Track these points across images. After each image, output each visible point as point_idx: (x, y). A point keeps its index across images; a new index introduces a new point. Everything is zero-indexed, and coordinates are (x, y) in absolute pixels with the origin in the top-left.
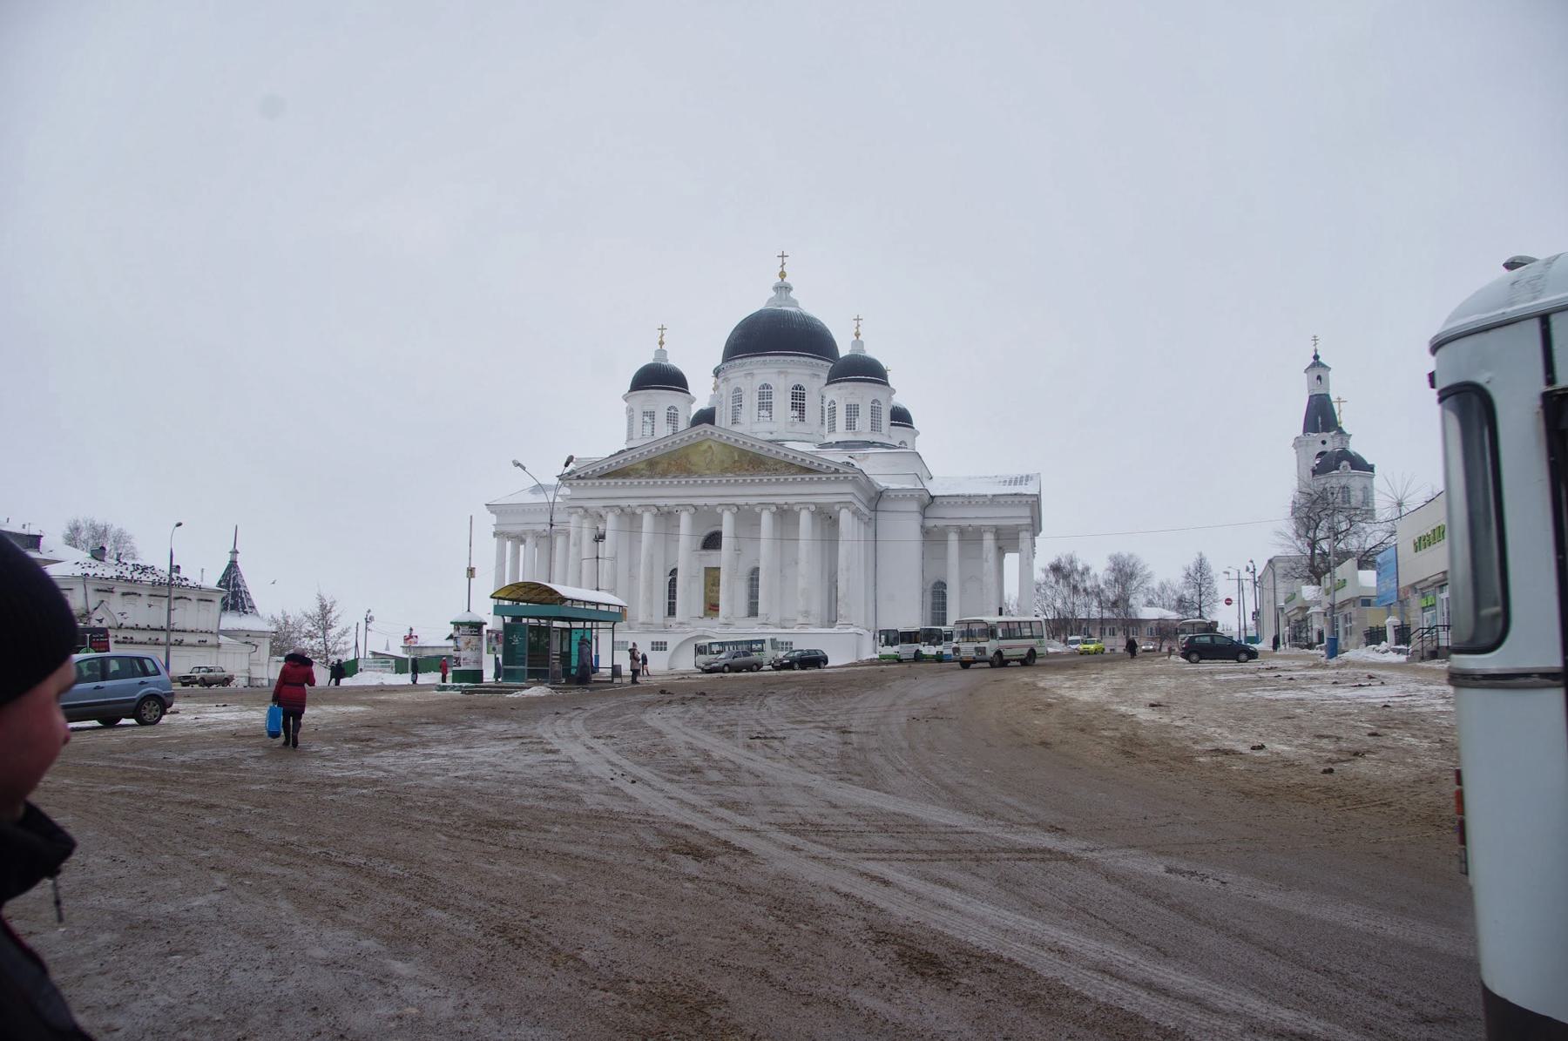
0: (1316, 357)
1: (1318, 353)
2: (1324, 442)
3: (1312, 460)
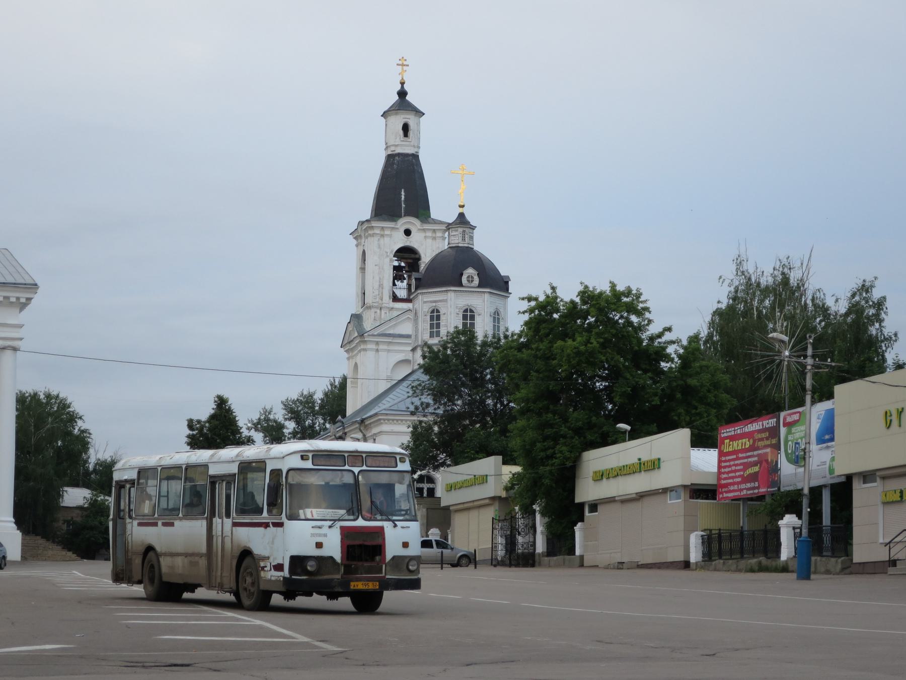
0: (402, 94)
2: (408, 233)
3: (388, 260)
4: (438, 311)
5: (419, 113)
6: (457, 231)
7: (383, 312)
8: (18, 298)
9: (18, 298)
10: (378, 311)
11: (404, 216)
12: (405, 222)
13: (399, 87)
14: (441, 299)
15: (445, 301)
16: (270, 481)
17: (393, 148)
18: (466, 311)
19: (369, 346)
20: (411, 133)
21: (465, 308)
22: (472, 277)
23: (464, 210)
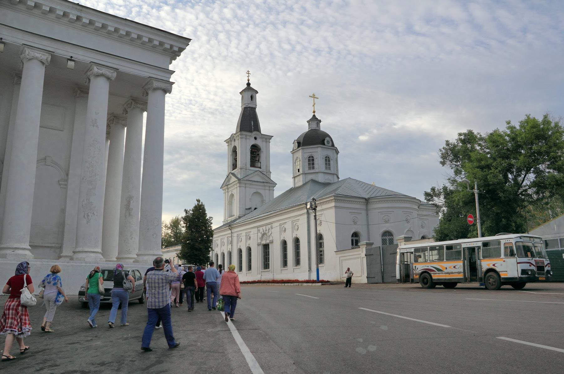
0: (249, 84)
1: (250, 82)
4: (312, 157)
5: (257, 92)
6: (315, 122)
7: (247, 171)
8: (172, 46)
9: (172, 46)
10: (245, 170)
11: (254, 131)
12: (255, 134)
13: (247, 82)
14: (313, 151)
15: (317, 152)
16: (118, 254)
17: (247, 105)
18: (326, 157)
19: (242, 185)
20: (254, 99)
21: (326, 156)
22: (329, 141)
23: (315, 114)
